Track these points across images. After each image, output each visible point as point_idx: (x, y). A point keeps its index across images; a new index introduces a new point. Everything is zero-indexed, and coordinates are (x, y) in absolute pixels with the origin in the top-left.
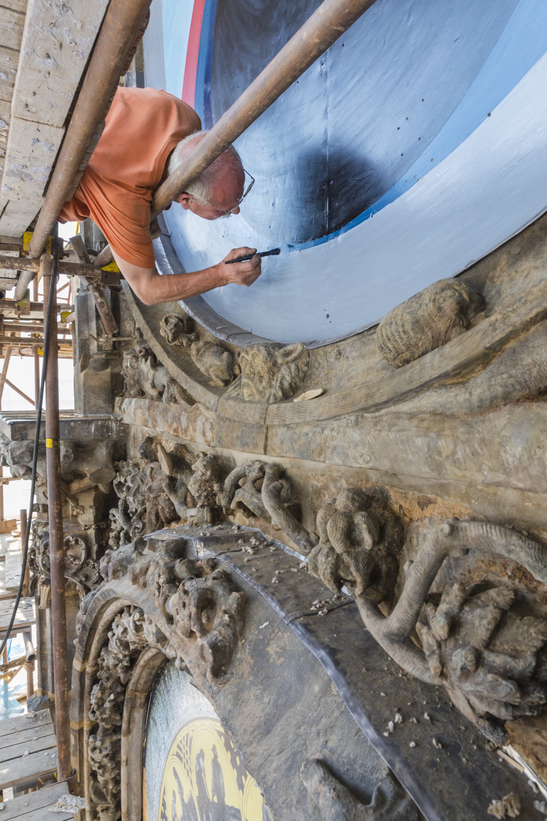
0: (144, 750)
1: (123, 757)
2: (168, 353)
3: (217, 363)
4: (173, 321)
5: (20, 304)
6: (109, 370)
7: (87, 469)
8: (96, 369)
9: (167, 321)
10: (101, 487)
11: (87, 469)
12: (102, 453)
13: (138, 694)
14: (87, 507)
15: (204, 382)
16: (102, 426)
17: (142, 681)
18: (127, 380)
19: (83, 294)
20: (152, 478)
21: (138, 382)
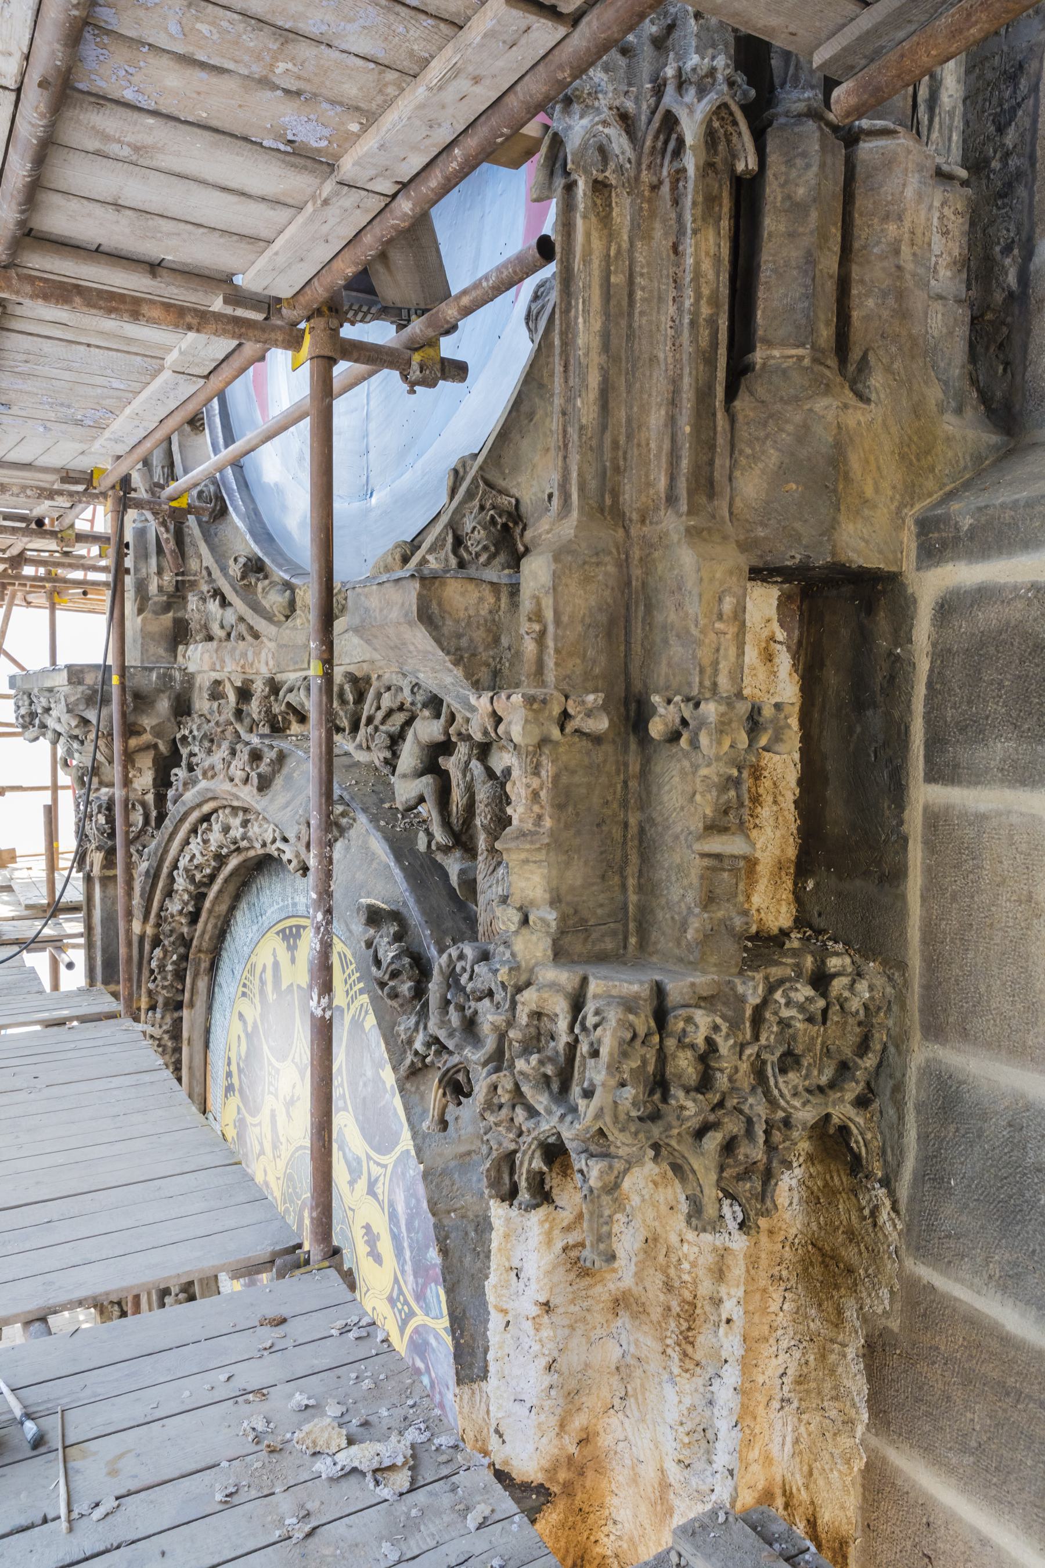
0: (208, 1031)
1: (185, 1035)
2: (236, 592)
3: (280, 599)
4: (242, 560)
5: (64, 534)
6: (171, 614)
7: (147, 722)
8: (156, 613)
9: (236, 560)
10: (162, 747)
11: (147, 722)
12: (164, 704)
13: (202, 956)
14: (144, 768)
15: (269, 618)
16: (165, 675)
17: (207, 937)
18: (193, 625)
19: (140, 525)
20: (220, 713)
21: (206, 627)
